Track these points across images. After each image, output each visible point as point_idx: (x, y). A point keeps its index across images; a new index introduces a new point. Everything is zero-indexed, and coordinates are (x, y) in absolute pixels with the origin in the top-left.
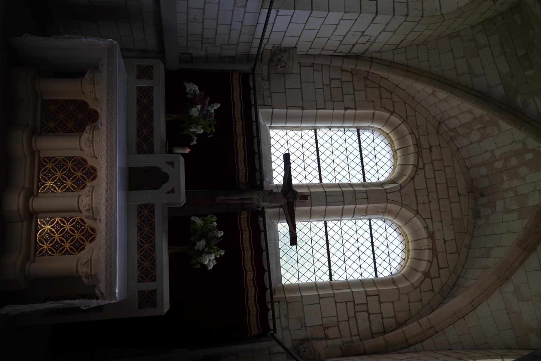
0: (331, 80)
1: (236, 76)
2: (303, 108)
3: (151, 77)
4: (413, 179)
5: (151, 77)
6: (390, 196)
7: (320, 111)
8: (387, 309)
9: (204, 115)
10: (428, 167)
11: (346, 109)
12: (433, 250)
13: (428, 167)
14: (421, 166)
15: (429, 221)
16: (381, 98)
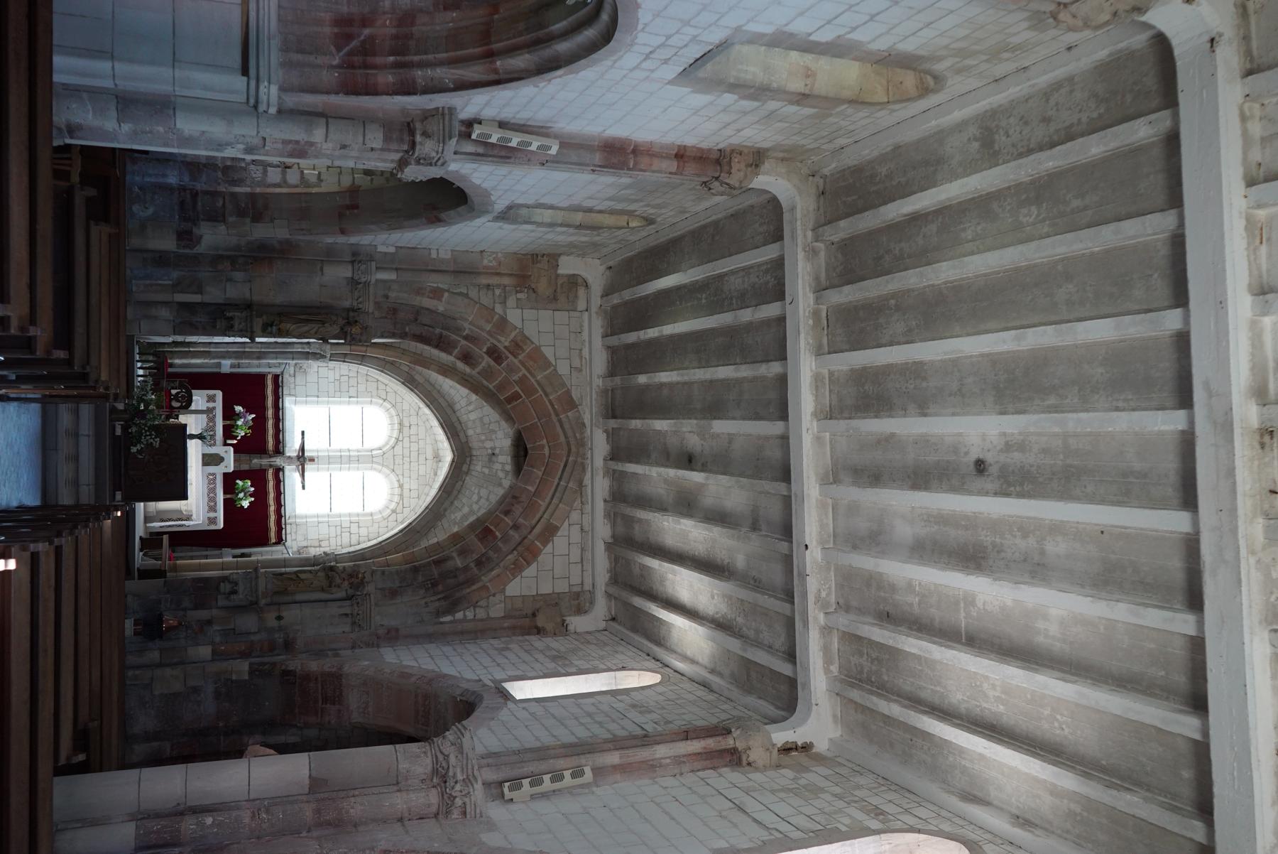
0: (341, 376)
1: (270, 377)
2: (318, 397)
3: (214, 401)
4: (393, 448)
5: (214, 401)
6: (374, 459)
7: (330, 399)
8: (363, 532)
9: (246, 423)
10: (406, 440)
11: (350, 397)
12: (401, 495)
13: (406, 440)
14: (401, 438)
15: (401, 477)
16: (378, 389)
